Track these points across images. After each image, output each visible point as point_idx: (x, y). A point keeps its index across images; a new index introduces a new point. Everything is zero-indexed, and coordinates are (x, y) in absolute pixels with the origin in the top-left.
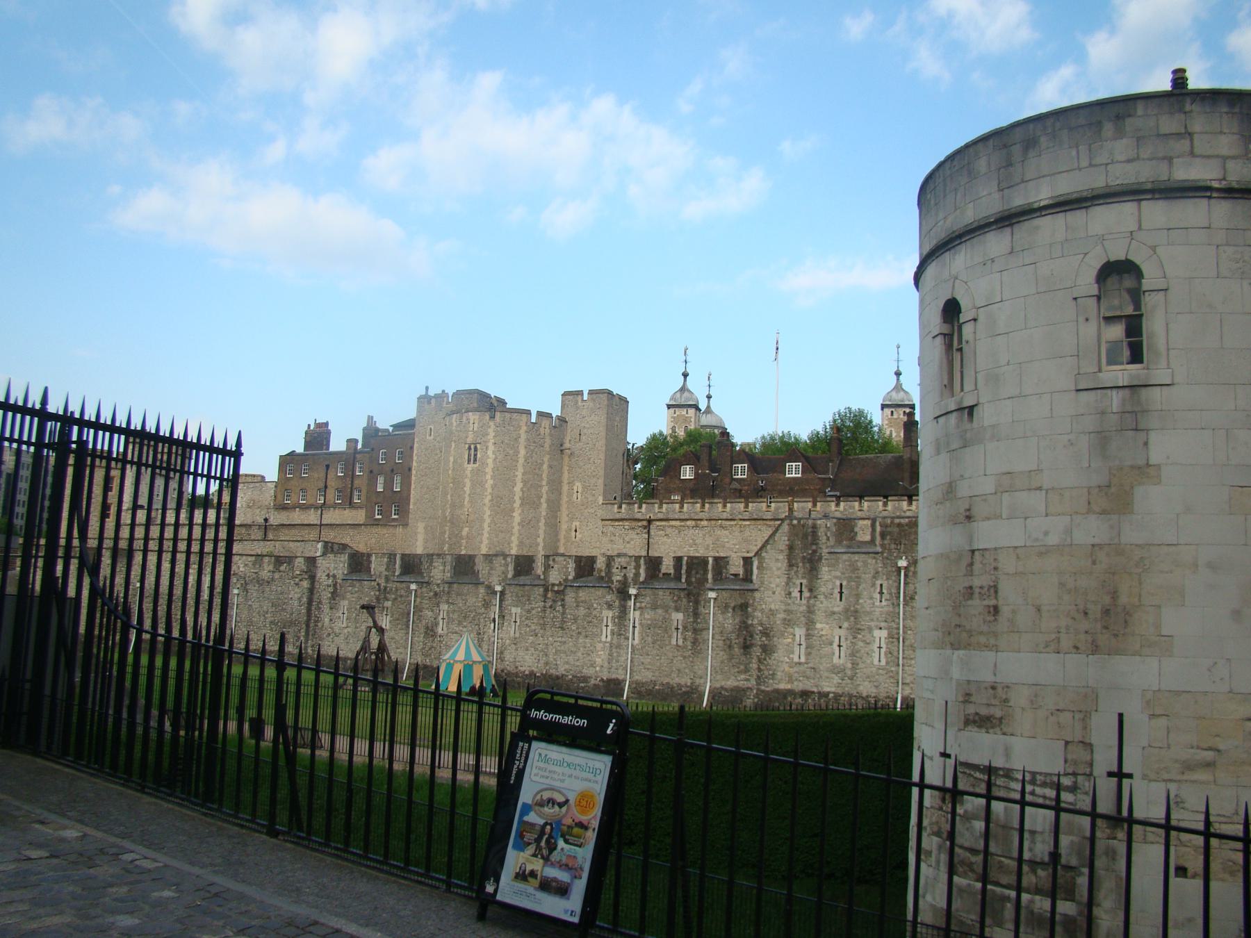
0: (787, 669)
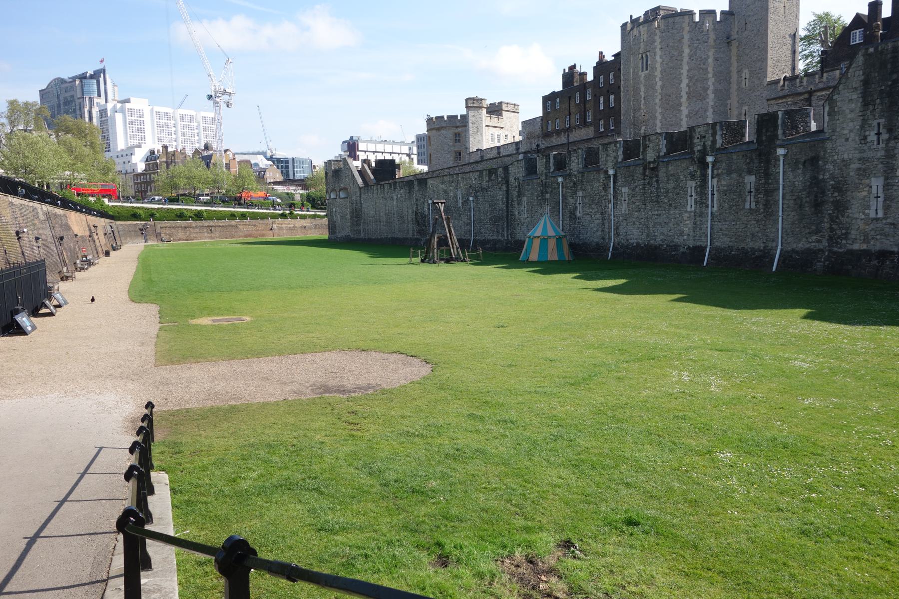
0: (862, 226)
